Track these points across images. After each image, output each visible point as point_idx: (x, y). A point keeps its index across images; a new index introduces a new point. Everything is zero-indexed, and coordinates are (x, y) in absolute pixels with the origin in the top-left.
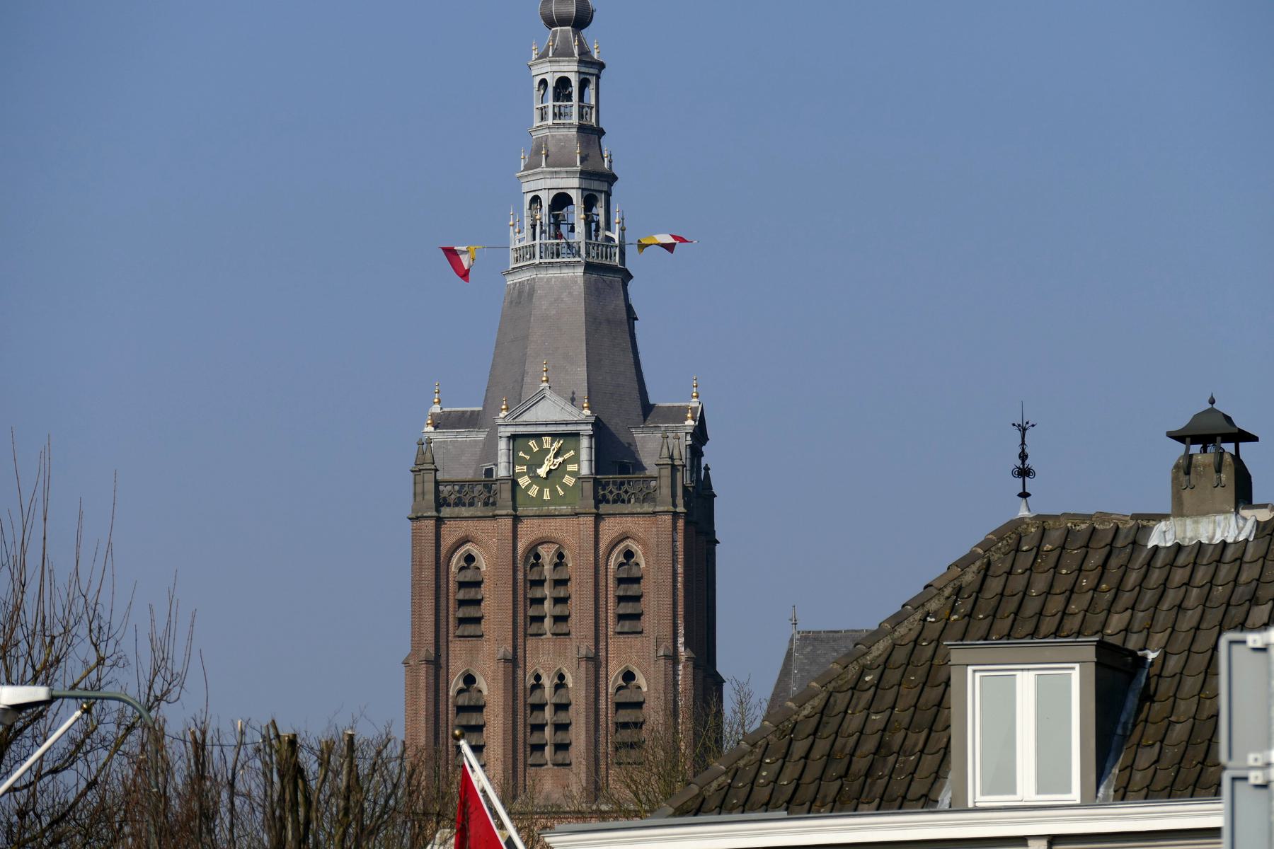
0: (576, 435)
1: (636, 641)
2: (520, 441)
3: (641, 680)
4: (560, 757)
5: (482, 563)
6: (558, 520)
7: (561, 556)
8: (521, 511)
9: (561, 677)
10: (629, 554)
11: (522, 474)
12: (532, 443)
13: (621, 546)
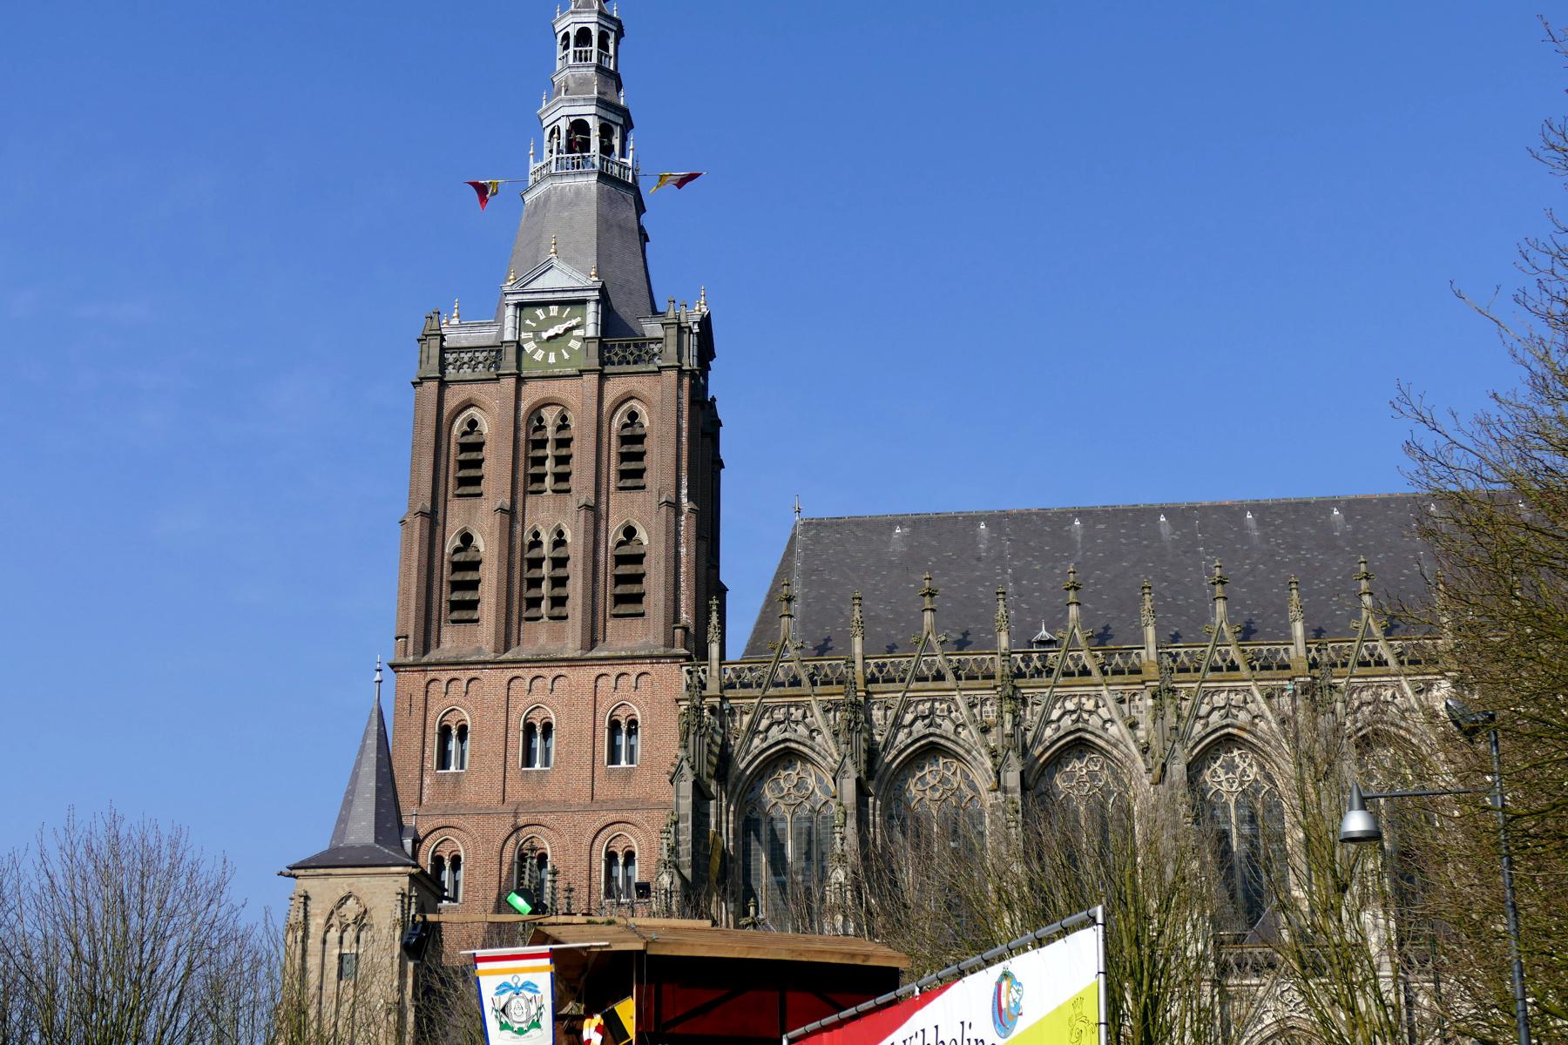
0: (583, 302)
1: (638, 496)
2: (527, 311)
3: (642, 535)
4: (557, 611)
5: (485, 427)
6: (562, 382)
7: (564, 418)
8: (525, 373)
9: (561, 533)
10: (633, 416)
11: (528, 340)
12: (539, 312)
13: (625, 406)
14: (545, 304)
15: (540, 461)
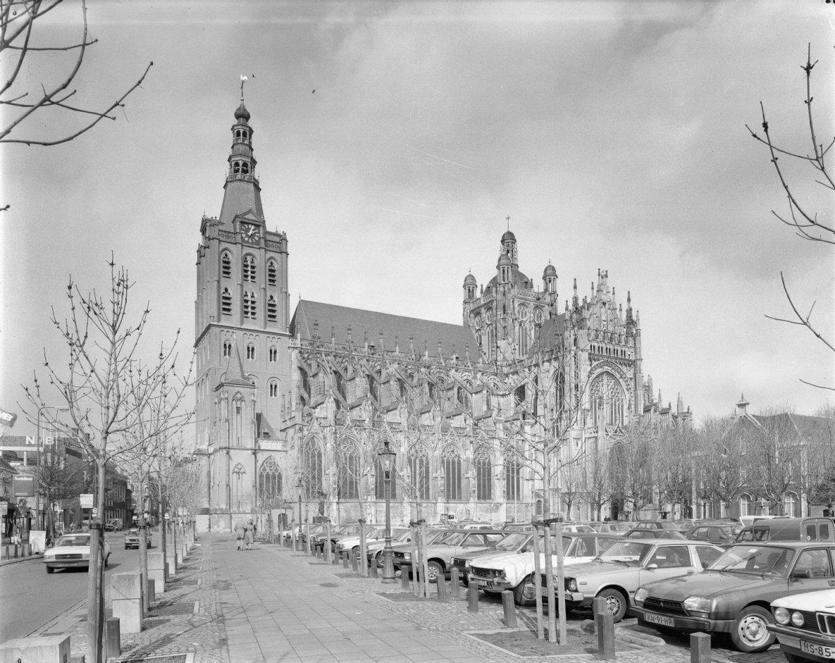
4: (253, 317)
14: (248, 224)
15: (246, 271)
